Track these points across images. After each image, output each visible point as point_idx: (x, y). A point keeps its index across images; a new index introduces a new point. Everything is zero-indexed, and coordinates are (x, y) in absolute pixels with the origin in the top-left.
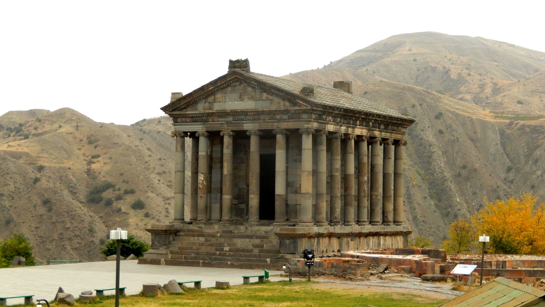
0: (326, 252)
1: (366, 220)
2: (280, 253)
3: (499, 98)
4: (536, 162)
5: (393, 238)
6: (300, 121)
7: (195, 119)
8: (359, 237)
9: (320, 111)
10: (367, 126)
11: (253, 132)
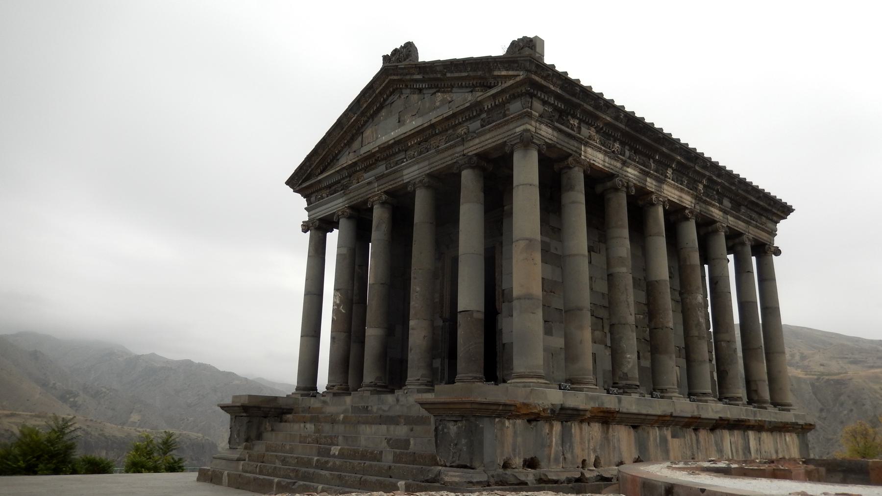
0: (596, 464)
1: (710, 391)
2: (437, 464)
3: (806, 363)
4: (842, 404)
5: (777, 436)
6: (507, 123)
7: (332, 188)
8: (696, 430)
9: (558, 97)
10: (692, 186)
11: (418, 180)
